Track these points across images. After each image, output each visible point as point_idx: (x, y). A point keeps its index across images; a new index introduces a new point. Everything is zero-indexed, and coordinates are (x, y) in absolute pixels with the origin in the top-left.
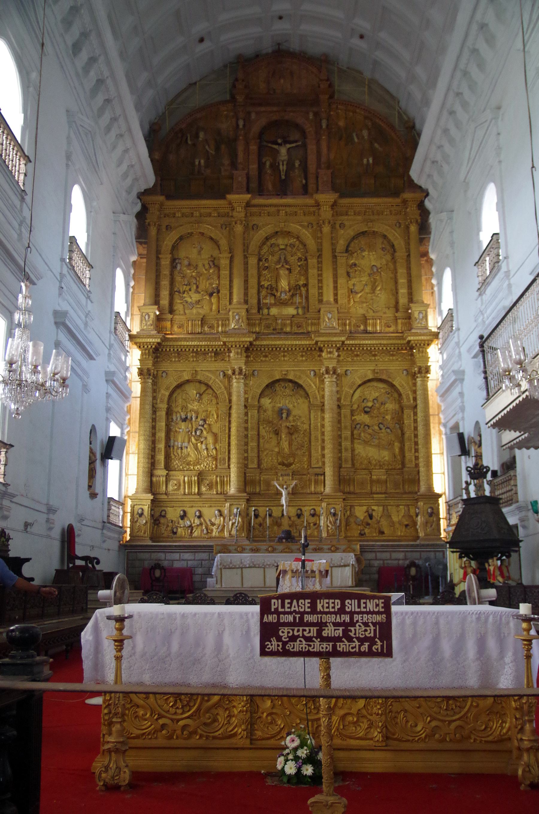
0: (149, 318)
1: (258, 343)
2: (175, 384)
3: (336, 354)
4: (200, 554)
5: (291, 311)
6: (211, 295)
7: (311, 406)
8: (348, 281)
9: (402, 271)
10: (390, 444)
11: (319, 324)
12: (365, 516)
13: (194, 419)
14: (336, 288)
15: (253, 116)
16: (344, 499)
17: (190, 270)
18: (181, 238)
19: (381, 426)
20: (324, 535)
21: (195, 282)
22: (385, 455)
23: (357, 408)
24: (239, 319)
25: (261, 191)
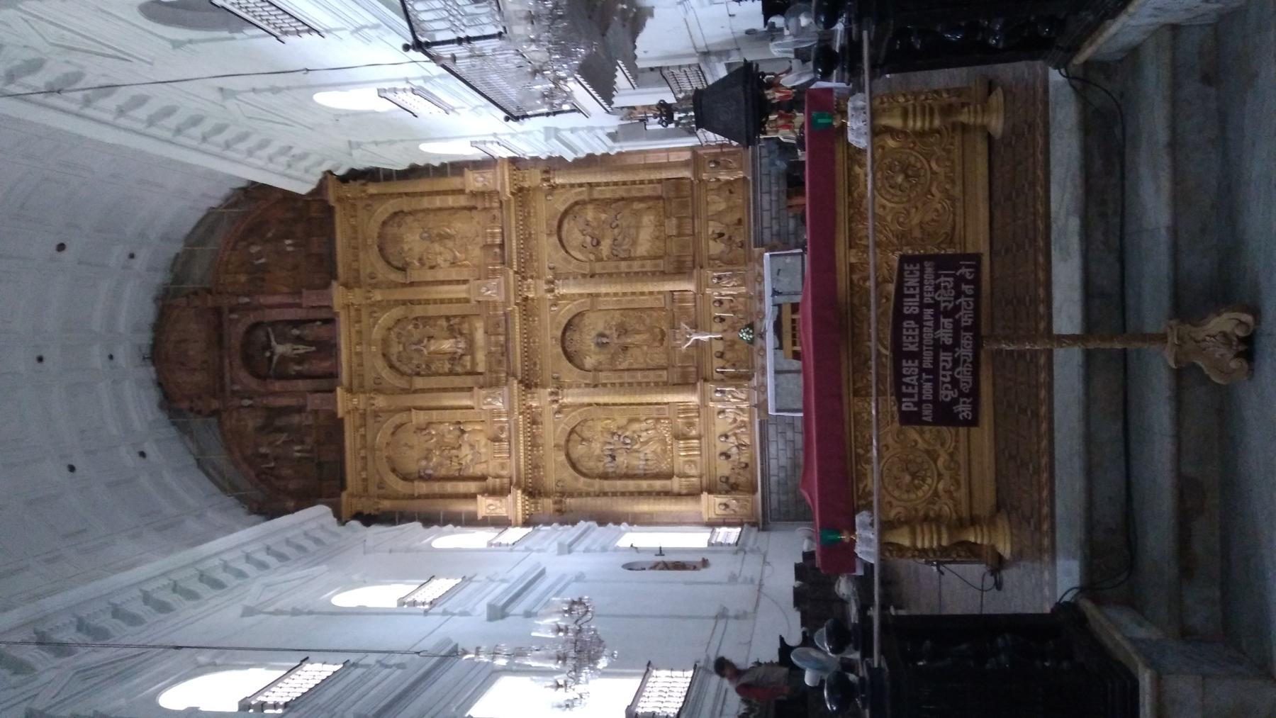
0: (491, 505)
2: (571, 470)
3: (530, 280)
4: (770, 435)
5: (480, 336)
6: (463, 432)
7: (592, 309)
9: (426, 203)
10: (637, 214)
11: (495, 302)
12: (723, 242)
13: (612, 447)
14: (450, 282)
15: (236, 387)
16: (701, 267)
17: (431, 460)
18: (394, 470)
19: (614, 225)
20: (743, 290)
21: (447, 452)
22: (648, 220)
23: (594, 254)
24: (490, 397)
25: (333, 376)
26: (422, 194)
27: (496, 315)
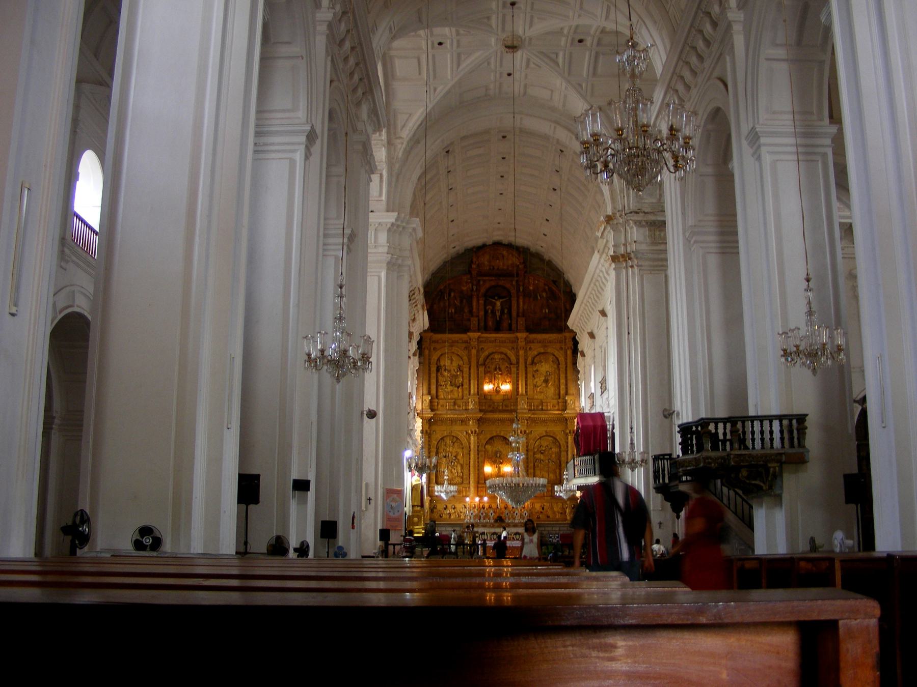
1: (484, 416)
3: (526, 422)
8: (533, 380)
9: (562, 376)
14: (526, 385)
15: (481, 283)
18: (442, 355)
19: (550, 461)
25: (486, 329)
26: (566, 373)
27: (511, 405)
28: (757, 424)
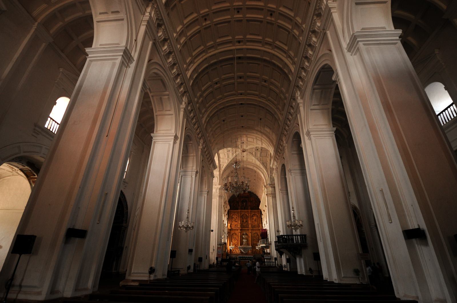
5: (245, 224)
9: (259, 219)
14: (251, 222)
25: (242, 209)
28: (294, 236)
